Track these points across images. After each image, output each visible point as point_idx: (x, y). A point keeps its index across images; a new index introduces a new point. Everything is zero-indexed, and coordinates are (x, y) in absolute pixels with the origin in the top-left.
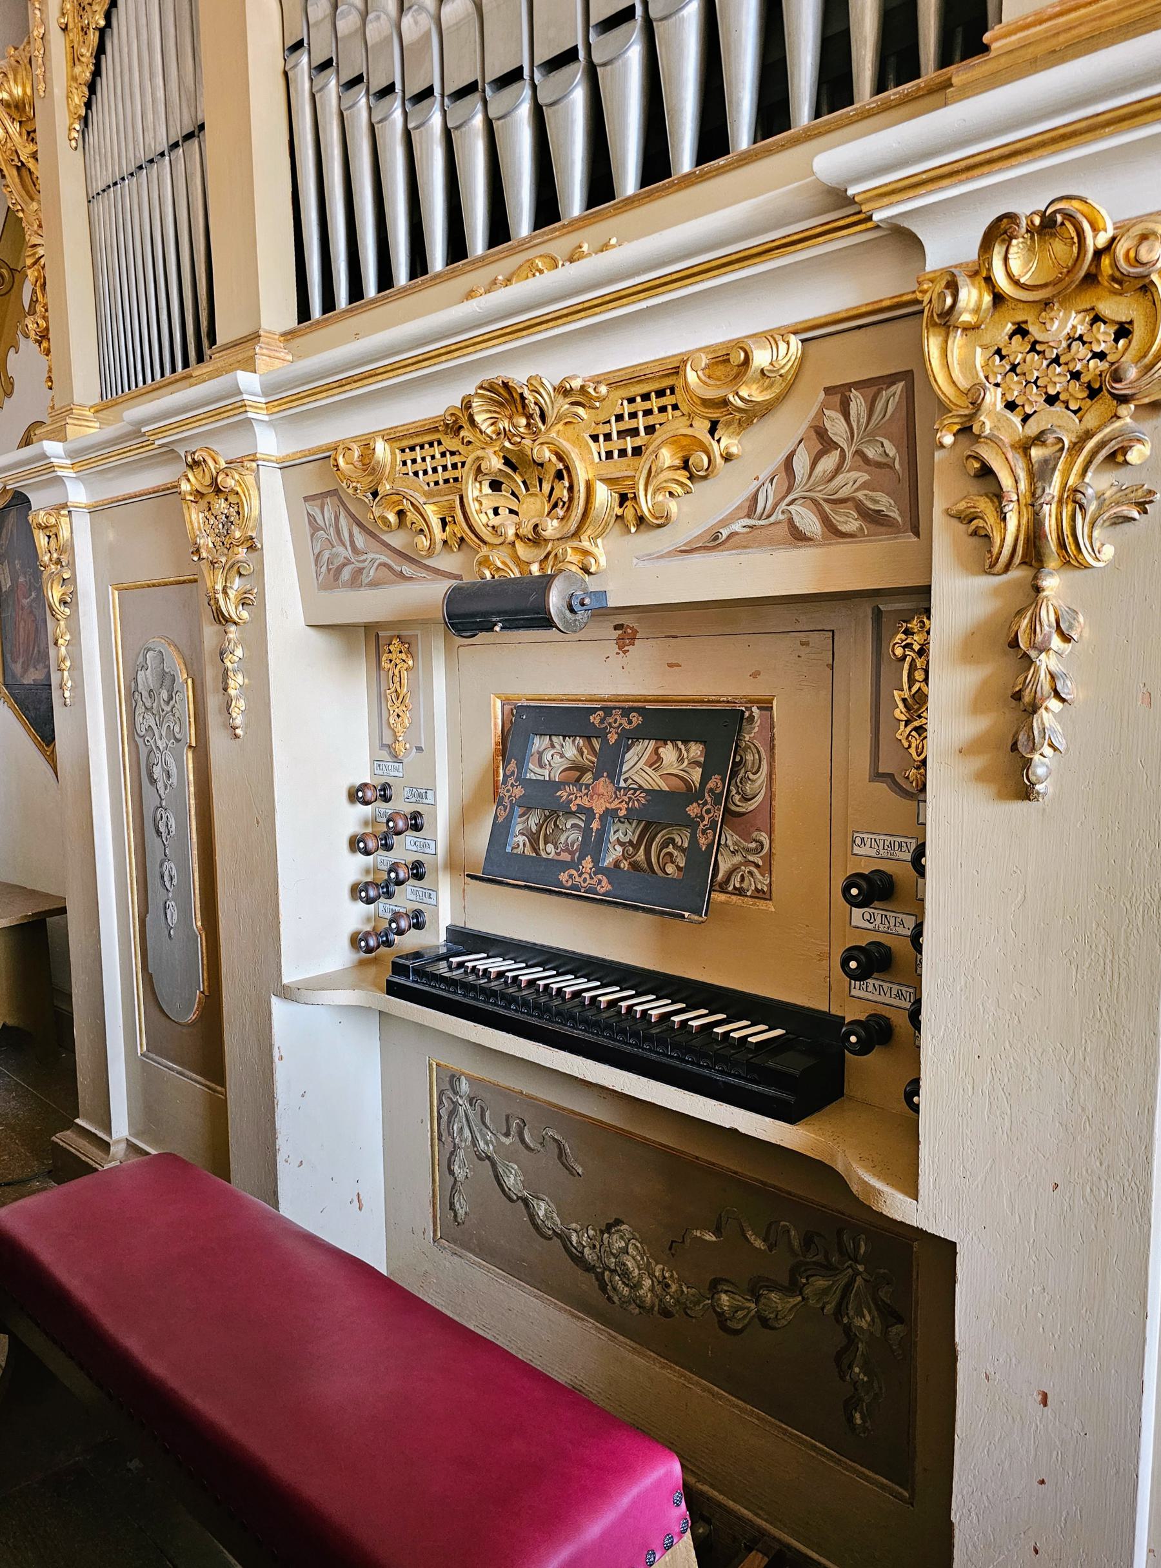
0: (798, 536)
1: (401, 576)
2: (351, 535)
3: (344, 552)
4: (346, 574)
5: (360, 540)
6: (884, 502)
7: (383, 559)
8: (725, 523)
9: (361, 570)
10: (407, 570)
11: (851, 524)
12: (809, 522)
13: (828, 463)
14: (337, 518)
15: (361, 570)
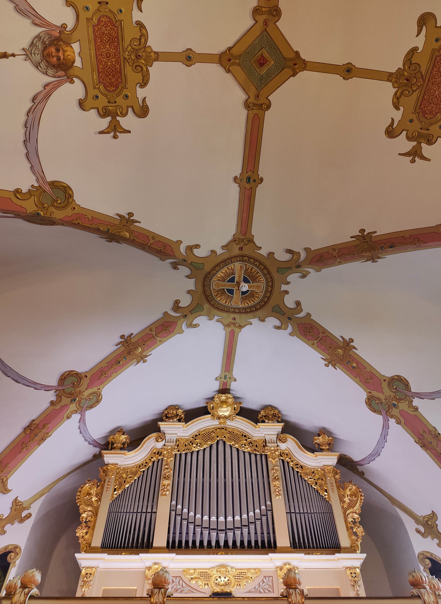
0: (261, 592)
1: (193, 592)
2: (182, 584)
3: (179, 587)
4: (179, 591)
5: (184, 585)
6: (270, 590)
7: (189, 589)
8: (252, 589)
9: (183, 591)
10: (194, 591)
11: (267, 592)
12: (262, 591)
13: (264, 584)
14: (179, 581)
15: (183, 591)
